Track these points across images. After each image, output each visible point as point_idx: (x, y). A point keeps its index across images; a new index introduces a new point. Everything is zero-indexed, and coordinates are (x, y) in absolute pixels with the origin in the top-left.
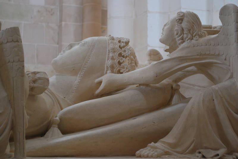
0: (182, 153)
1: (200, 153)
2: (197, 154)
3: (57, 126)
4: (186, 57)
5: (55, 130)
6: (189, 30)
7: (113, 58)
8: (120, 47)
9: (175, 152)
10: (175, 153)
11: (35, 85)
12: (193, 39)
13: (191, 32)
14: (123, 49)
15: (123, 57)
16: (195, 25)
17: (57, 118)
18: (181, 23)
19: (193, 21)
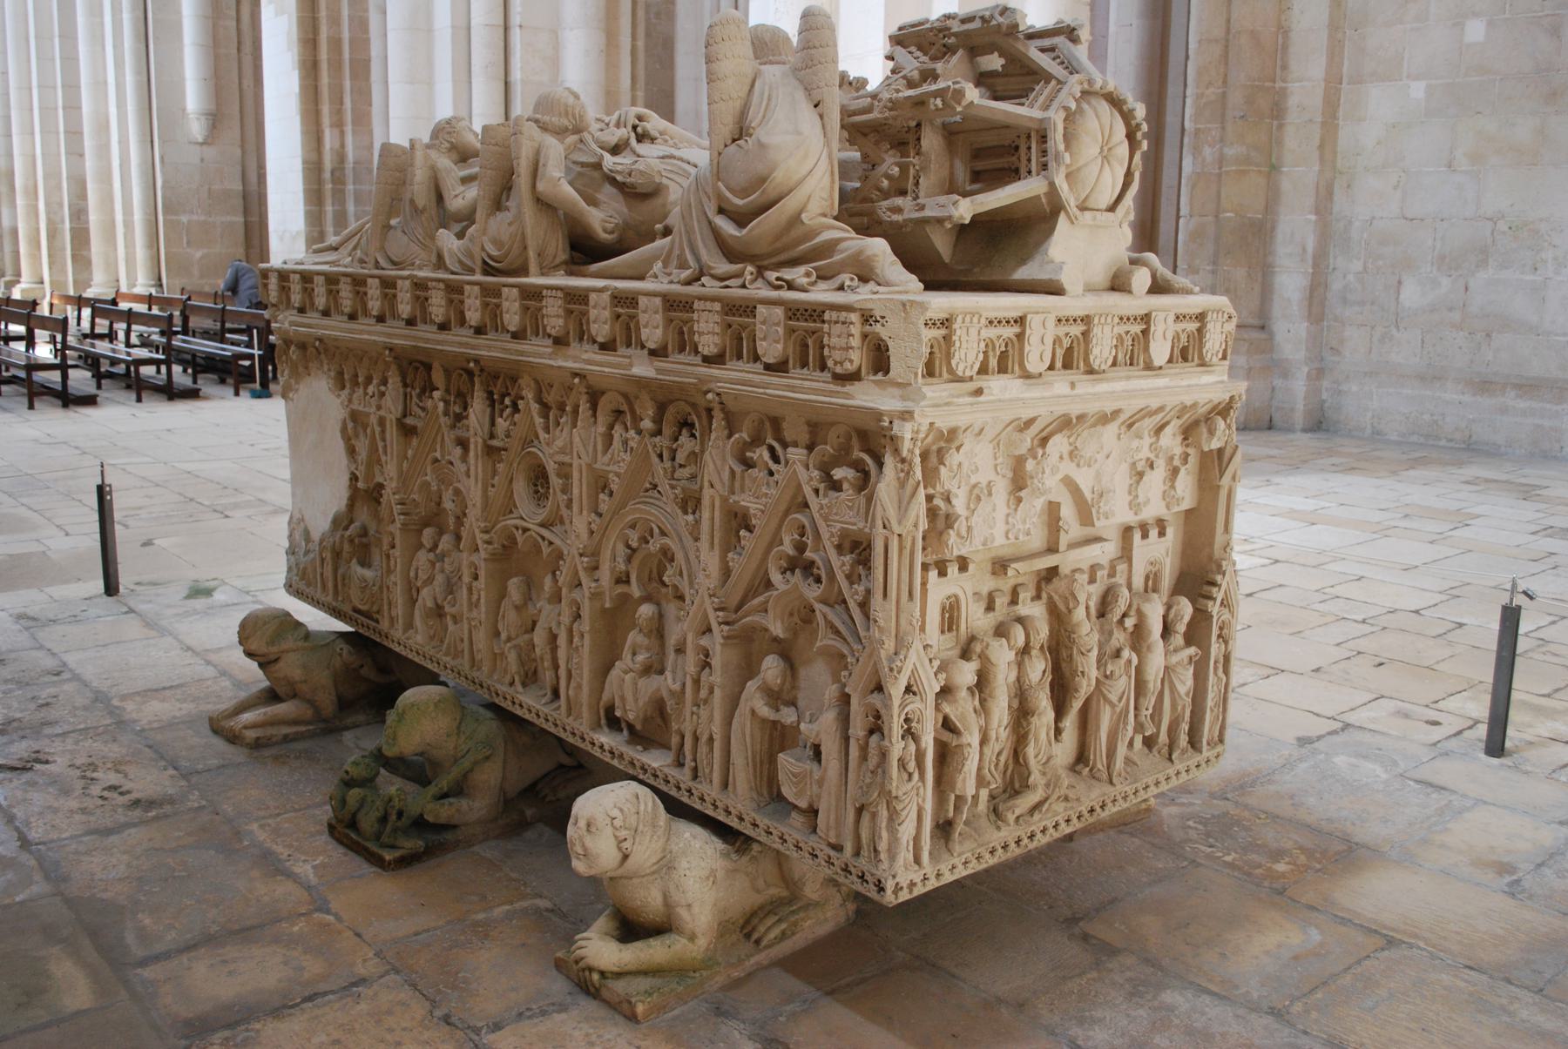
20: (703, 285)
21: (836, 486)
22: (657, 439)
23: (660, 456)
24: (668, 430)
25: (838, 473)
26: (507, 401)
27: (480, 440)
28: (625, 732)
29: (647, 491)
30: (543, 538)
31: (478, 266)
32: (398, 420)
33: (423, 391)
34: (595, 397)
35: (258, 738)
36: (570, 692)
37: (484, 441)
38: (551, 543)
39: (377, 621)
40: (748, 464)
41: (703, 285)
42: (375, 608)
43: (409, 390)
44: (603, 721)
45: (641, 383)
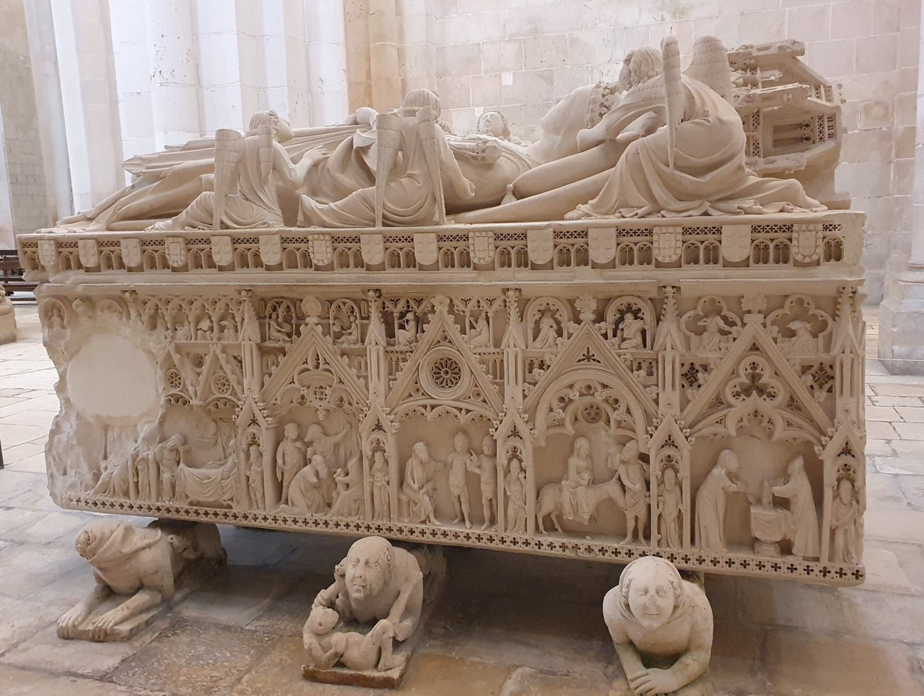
0: (606, 214)
1: (620, 212)
2: (617, 215)
3: (511, 193)
4: (631, 103)
5: (509, 196)
6: (635, 72)
7: (593, 111)
8: (604, 96)
9: (596, 213)
10: (595, 214)
11: (484, 155)
12: (640, 82)
13: (638, 73)
14: (606, 97)
15: (606, 107)
16: (644, 65)
17: (511, 185)
18: (628, 64)
19: (642, 60)
20: (663, 216)
21: (793, 334)
22: (602, 324)
23: (605, 336)
24: (611, 316)
25: (794, 325)
26: (410, 316)
27: (381, 348)
28: (559, 530)
29: (580, 361)
30: (460, 410)
31: (379, 221)
32: (258, 345)
33: (287, 320)
34: (523, 304)
35: (131, 630)
36: (511, 512)
37: (384, 348)
38: (468, 411)
39: (230, 507)
40: (700, 332)
41: (663, 216)
42: (226, 497)
43: (267, 320)
44: (541, 527)
45: (584, 288)
